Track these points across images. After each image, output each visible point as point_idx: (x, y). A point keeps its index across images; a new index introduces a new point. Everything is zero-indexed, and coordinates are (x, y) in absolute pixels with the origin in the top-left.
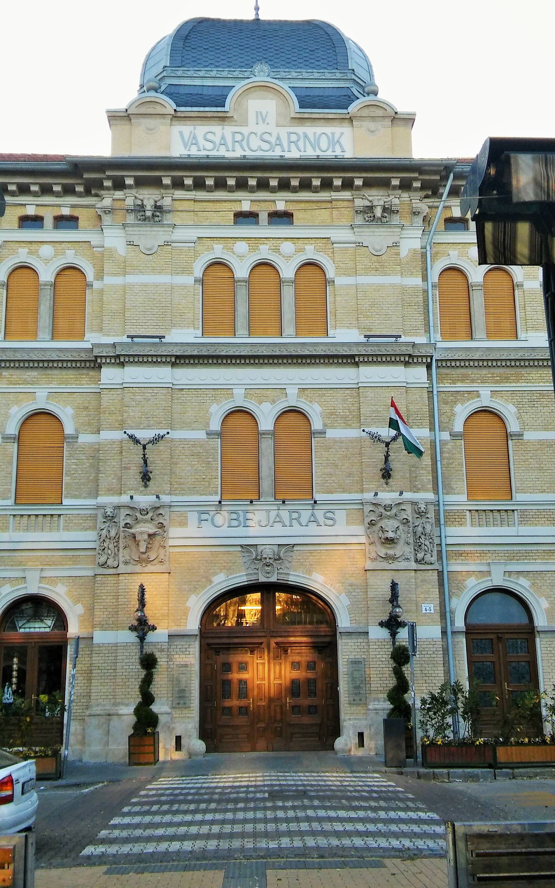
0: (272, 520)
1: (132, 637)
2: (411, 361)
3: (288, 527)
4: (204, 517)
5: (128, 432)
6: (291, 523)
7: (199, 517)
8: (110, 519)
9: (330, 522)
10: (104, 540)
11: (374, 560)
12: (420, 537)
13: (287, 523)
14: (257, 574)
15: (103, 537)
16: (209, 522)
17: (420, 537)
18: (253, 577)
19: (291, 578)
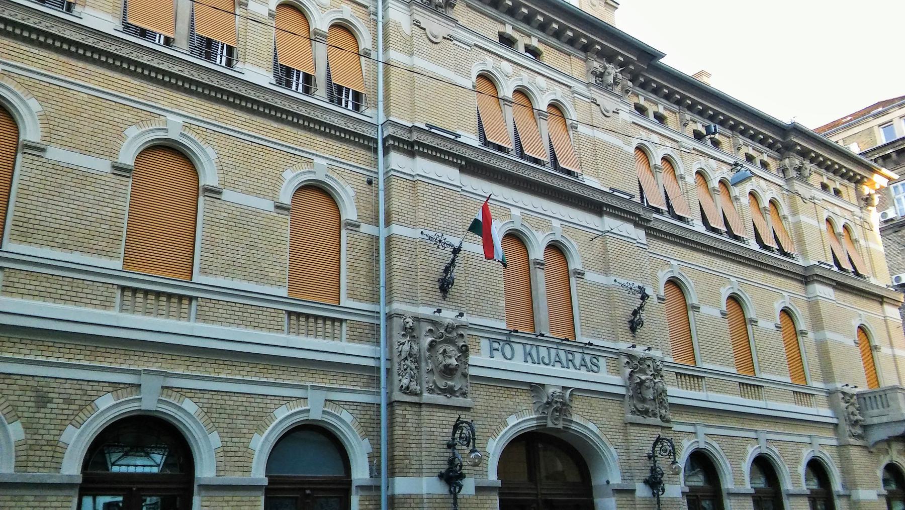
0: (552, 360)
1: (437, 488)
2: (640, 222)
3: (565, 369)
4: (496, 345)
5: (425, 232)
6: (568, 364)
7: (491, 346)
8: (410, 332)
9: (595, 368)
10: (406, 359)
11: (633, 413)
12: (661, 394)
13: (565, 365)
14: (546, 418)
15: (404, 355)
16: (500, 353)
17: (661, 394)
18: (542, 422)
19: (574, 427)
